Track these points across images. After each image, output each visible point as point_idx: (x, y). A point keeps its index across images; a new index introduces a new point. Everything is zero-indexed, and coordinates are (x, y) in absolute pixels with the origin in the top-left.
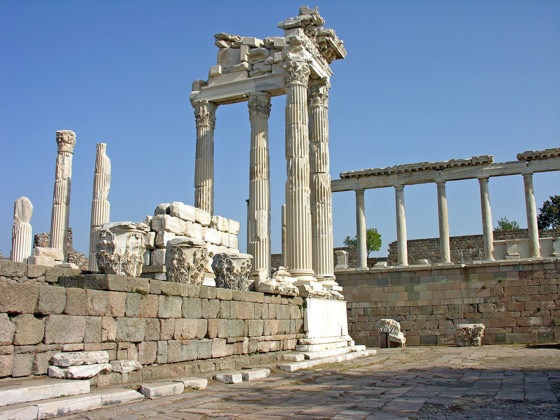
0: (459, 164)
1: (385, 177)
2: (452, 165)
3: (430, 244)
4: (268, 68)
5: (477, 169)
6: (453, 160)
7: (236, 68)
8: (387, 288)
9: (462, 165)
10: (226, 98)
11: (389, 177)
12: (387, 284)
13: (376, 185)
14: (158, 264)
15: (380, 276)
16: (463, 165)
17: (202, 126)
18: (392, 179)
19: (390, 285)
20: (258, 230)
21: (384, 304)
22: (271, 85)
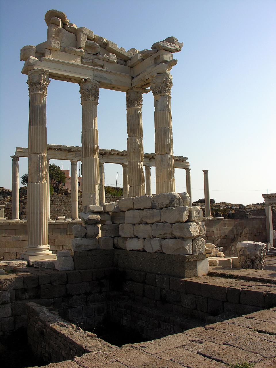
0: (116, 153)
1: (66, 152)
2: (112, 153)
3: (54, 200)
4: (101, 63)
5: (124, 158)
6: (114, 150)
7: (75, 51)
8: (66, 236)
9: (118, 154)
10: (64, 76)
11: (69, 153)
12: (67, 232)
13: (60, 158)
14: (200, 252)
15: (62, 227)
16: (118, 154)
17: (42, 94)
18: (71, 155)
19: (68, 233)
20: (97, 201)
21: (64, 247)
22: (106, 79)
